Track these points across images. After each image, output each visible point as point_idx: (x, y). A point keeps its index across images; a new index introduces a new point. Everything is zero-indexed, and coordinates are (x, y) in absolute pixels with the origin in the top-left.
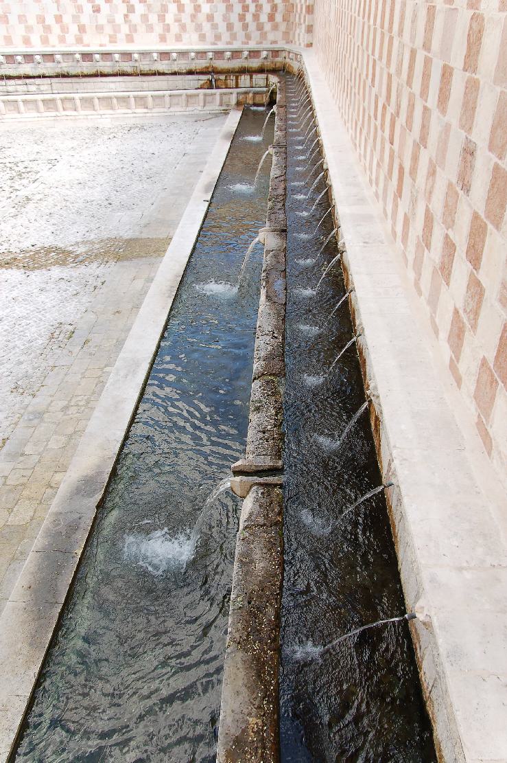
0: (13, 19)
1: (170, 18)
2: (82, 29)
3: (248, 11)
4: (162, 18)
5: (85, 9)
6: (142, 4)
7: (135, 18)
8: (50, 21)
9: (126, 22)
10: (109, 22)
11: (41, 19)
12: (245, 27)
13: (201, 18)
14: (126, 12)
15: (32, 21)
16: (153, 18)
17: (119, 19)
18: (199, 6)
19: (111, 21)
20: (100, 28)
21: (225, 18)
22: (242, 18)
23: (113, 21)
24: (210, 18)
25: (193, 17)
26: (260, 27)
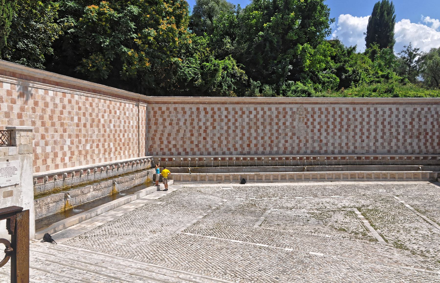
0: (329, 144)
1: (393, 144)
2: (355, 148)
3: (428, 142)
4: (389, 144)
5: (358, 141)
6: (382, 139)
7: (378, 144)
8: (343, 144)
9: (374, 145)
10: (367, 145)
11: (340, 144)
12: (426, 147)
13: (407, 144)
14: (374, 142)
15: (336, 145)
16: (386, 144)
17: (371, 144)
18: (406, 140)
19: (368, 145)
20: (363, 148)
21: (417, 144)
22: (425, 144)
23: (369, 145)
24: (410, 144)
25: (403, 144)
26: (433, 147)
